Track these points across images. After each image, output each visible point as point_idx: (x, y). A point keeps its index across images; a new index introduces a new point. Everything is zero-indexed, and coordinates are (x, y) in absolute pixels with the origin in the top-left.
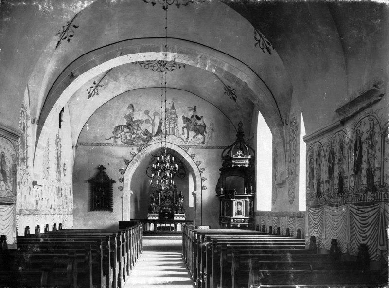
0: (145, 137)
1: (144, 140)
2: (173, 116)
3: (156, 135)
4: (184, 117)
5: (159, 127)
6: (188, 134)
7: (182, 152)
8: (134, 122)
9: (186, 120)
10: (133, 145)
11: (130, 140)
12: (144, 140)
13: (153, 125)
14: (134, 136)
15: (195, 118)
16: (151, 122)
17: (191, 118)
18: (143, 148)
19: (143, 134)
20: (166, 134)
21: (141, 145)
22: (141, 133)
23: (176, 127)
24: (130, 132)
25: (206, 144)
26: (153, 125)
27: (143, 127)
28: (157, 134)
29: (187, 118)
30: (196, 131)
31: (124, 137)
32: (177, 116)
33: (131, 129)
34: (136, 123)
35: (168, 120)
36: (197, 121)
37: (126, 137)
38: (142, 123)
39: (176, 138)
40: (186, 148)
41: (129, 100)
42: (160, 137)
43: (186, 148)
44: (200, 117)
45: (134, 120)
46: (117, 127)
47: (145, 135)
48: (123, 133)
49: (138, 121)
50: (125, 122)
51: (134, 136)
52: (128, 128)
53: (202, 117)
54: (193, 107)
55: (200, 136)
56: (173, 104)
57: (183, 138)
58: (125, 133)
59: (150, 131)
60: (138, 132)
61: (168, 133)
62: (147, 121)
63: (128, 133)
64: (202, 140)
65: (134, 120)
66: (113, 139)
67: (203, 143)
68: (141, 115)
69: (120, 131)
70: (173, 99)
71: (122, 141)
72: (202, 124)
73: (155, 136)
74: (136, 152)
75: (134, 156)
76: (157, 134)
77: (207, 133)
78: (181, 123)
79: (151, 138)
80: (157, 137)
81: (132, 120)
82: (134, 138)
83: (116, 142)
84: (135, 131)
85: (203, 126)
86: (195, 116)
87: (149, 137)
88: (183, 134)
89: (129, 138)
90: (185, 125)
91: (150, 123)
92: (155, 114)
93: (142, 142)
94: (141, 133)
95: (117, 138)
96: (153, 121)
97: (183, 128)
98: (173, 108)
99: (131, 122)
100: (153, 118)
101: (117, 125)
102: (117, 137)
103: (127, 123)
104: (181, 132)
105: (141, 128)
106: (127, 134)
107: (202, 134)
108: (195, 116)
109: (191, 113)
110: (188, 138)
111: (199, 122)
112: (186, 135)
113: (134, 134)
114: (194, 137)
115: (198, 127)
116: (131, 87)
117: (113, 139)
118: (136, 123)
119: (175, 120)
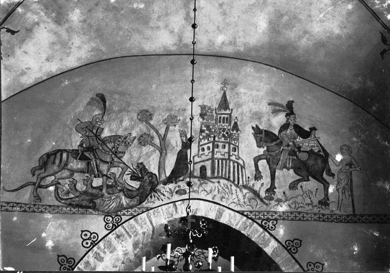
0: (136, 184)
1: (129, 193)
2: (225, 125)
3: (169, 180)
4: (257, 131)
5: (182, 160)
6: (273, 178)
7: (255, 233)
8: (104, 142)
9: (263, 136)
10: (94, 208)
11: (85, 193)
12: (129, 193)
13: (163, 149)
14: (97, 182)
15: (290, 131)
16: (157, 141)
17: (280, 131)
18: (124, 218)
19: (127, 178)
20: (203, 176)
21: (121, 208)
22: (122, 174)
23: (233, 158)
24: (88, 170)
25: (333, 207)
26: (163, 149)
27: (132, 155)
28: (173, 177)
29: (268, 133)
30: (297, 171)
31: (66, 185)
32: (236, 127)
33: (93, 163)
34: (110, 146)
35: (208, 136)
36: (299, 140)
37: (74, 184)
38: (127, 145)
39: (234, 188)
40: (268, 220)
41: (96, 84)
42: (183, 185)
43: (268, 220)
44: (307, 129)
45: (103, 136)
46: (48, 155)
47: (134, 178)
48: (66, 173)
49: (115, 138)
50: (76, 141)
51: (97, 182)
52: (83, 158)
53: (313, 129)
54: (285, 104)
55: (312, 184)
56: (224, 94)
57: (256, 188)
58: (73, 172)
59: (153, 169)
60: (113, 170)
61: (209, 173)
62: (144, 140)
63: (82, 171)
64: (321, 196)
65: (103, 136)
66: (30, 189)
67: (324, 203)
68: (126, 123)
69: (55, 168)
70: (225, 83)
71: (58, 197)
72: (316, 150)
73: (165, 183)
74: (103, 232)
75: (94, 244)
76: (173, 177)
77: (333, 175)
78: (249, 148)
79: (154, 189)
80: (171, 186)
81: (97, 136)
82: (100, 188)
83: (38, 198)
84: (104, 168)
85: (317, 155)
86: (291, 127)
87: (147, 186)
88: (258, 176)
89: (80, 187)
90: (262, 151)
91: (153, 145)
92: (171, 120)
93: (124, 201)
94: (122, 174)
95: (40, 186)
96: (163, 139)
97: (257, 160)
98: (224, 103)
99: (94, 143)
100: (162, 131)
101: (49, 146)
102: (42, 183)
103: (81, 145)
104: (250, 171)
105: (125, 158)
106: (77, 176)
107: (319, 178)
108: (291, 127)
109: (279, 119)
110: (271, 190)
111: (307, 144)
112: (266, 180)
113: (100, 174)
114: (293, 186)
115: (303, 156)
116: (106, 52)
117: (30, 189)
118: (110, 146)
119: (230, 136)
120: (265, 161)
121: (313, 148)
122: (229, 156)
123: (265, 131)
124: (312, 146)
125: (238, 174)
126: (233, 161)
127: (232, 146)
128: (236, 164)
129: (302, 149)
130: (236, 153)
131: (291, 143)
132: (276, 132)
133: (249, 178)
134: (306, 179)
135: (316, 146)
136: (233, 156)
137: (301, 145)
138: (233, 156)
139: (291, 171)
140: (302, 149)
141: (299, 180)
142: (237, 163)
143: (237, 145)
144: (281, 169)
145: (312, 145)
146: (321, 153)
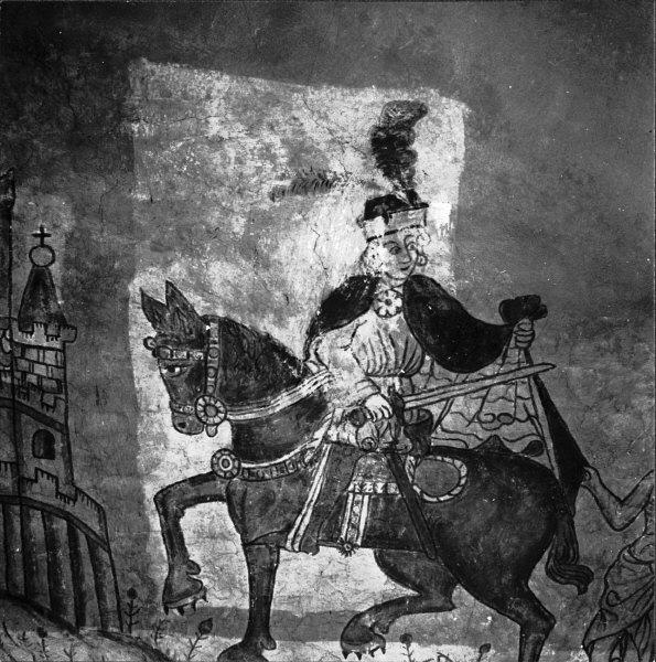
72: (517, 436)
85: (523, 466)
120: (223, 507)
121: (505, 431)
122: (21, 481)
123: (227, 325)
124: (507, 418)
125: (78, 578)
126: (48, 513)
127: (30, 428)
128: (61, 526)
129: (438, 438)
130: (56, 466)
131: (376, 403)
132: (291, 336)
133: (132, 594)
134: (438, 601)
135: (523, 416)
136: (43, 480)
137: (435, 410)
138: (43, 480)
139: (365, 558)
140: (438, 438)
141: (401, 601)
142: (68, 517)
143: (58, 417)
144: (308, 547)
145: (497, 408)
146: (547, 459)
